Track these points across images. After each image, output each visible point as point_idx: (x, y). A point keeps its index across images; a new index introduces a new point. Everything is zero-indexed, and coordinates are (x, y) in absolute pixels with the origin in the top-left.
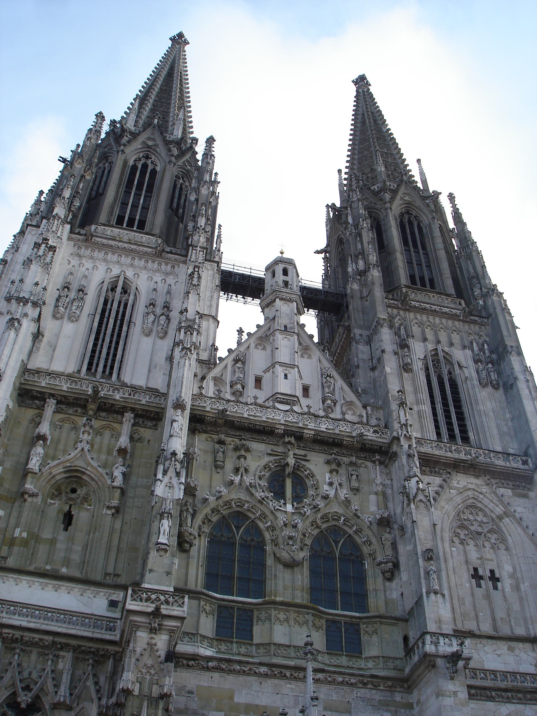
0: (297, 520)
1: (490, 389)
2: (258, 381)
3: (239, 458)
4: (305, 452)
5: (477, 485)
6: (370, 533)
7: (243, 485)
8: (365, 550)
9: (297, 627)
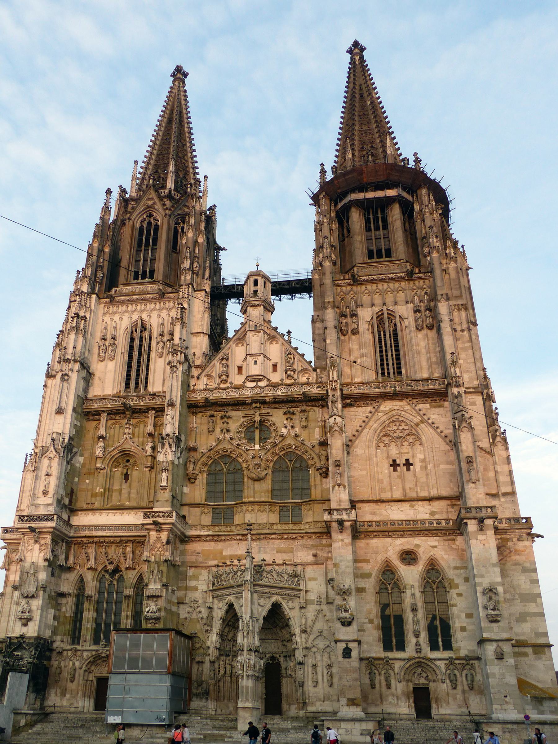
0: (262, 453)
1: (425, 331)
2: (240, 368)
3: (223, 423)
4: (269, 411)
5: (401, 406)
6: (312, 453)
7: (227, 440)
8: (310, 462)
9: (259, 513)
